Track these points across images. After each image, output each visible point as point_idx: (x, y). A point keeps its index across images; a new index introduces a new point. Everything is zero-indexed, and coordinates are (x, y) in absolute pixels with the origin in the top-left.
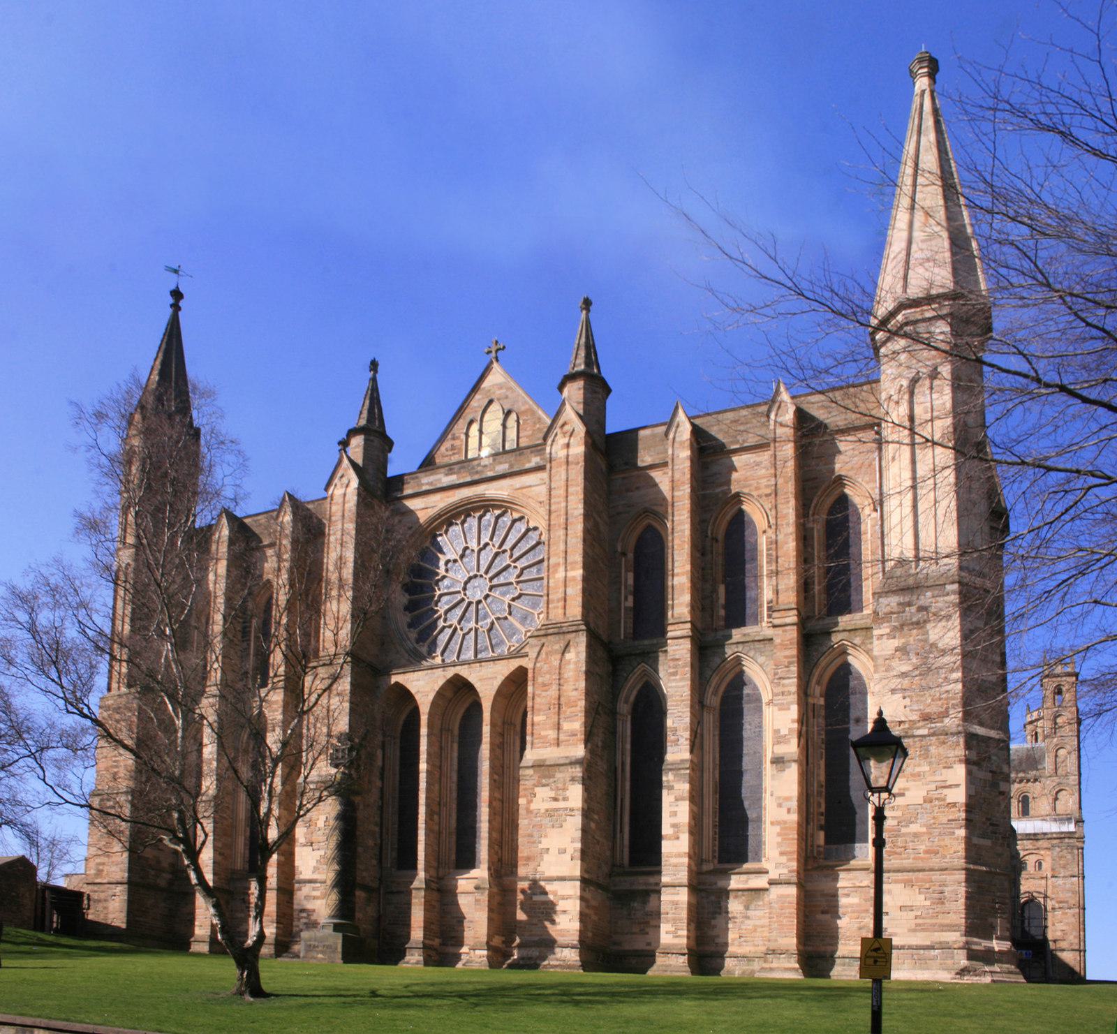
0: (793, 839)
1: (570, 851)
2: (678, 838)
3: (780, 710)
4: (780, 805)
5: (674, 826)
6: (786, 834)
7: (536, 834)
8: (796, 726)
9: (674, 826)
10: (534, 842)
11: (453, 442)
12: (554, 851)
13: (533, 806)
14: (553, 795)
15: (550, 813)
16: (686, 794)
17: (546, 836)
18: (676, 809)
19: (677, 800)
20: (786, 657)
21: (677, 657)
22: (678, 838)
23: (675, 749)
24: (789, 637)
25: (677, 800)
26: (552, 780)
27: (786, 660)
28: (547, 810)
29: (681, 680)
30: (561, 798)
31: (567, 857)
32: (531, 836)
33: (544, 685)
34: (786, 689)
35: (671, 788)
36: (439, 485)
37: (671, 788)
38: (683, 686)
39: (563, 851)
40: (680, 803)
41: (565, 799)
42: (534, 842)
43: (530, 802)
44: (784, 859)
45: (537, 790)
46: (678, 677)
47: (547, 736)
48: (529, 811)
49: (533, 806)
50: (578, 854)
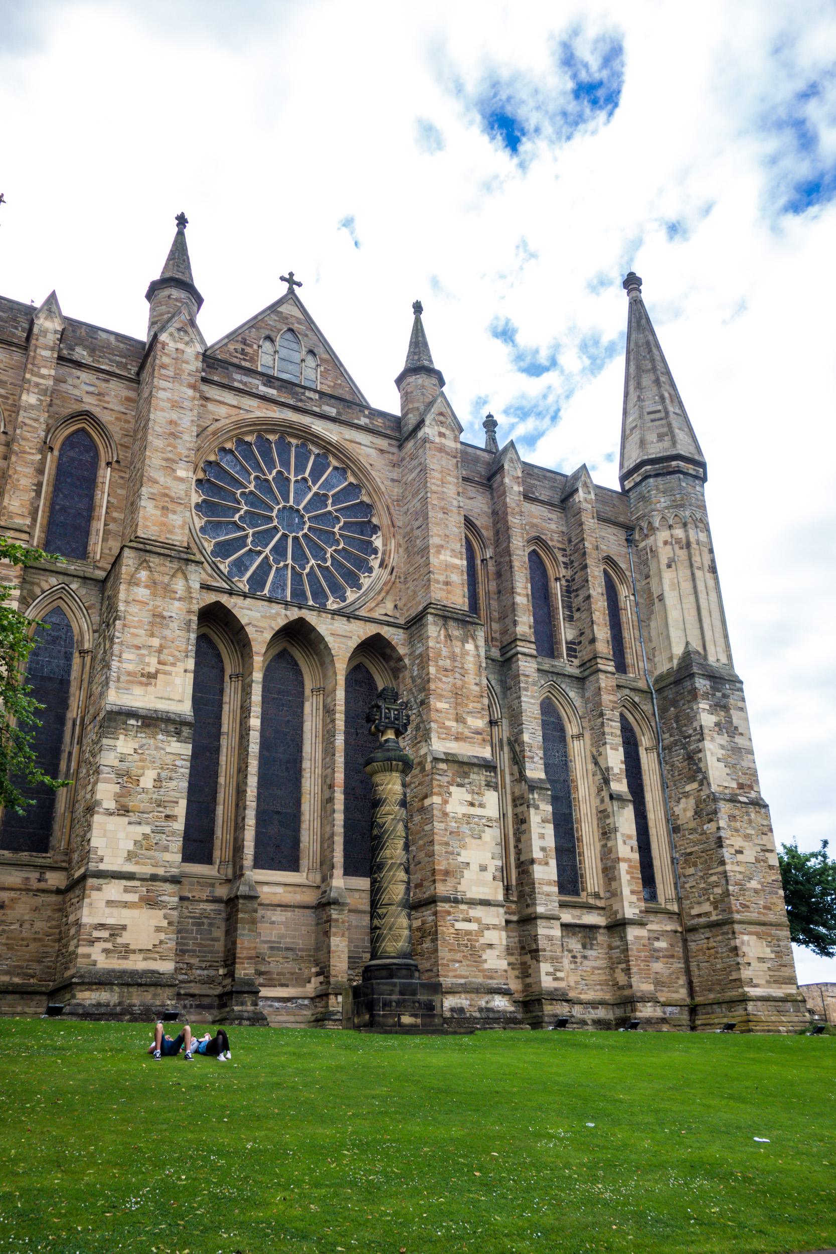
0: (638, 878)
1: (491, 869)
2: (547, 864)
3: (611, 748)
4: (625, 843)
5: (543, 849)
6: (632, 873)
7: (454, 843)
8: (623, 766)
9: (543, 849)
10: (452, 853)
11: (244, 347)
12: (474, 867)
13: (449, 808)
14: (470, 799)
15: (468, 817)
16: (550, 817)
17: (464, 847)
18: (543, 831)
19: (543, 821)
20: (610, 701)
21: (527, 673)
22: (547, 864)
23: (533, 766)
24: (611, 684)
25: (543, 821)
26: (467, 781)
27: (612, 704)
28: (464, 815)
29: (533, 697)
30: (477, 803)
31: (488, 875)
32: (447, 844)
33: (446, 670)
34: (614, 731)
35: (537, 808)
36: (254, 391)
37: (537, 808)
38: (534, 704)
39: (483, 868)
40: (547, 824)
41: (481, 805)
42: (452, 853)
43: (446, 802)
44: (634, 898)
45: (453, 789)
46: (529, 693)
47: (448, 728)
48: (445, 814)
49: (449, 808)
50: (498, 874)
